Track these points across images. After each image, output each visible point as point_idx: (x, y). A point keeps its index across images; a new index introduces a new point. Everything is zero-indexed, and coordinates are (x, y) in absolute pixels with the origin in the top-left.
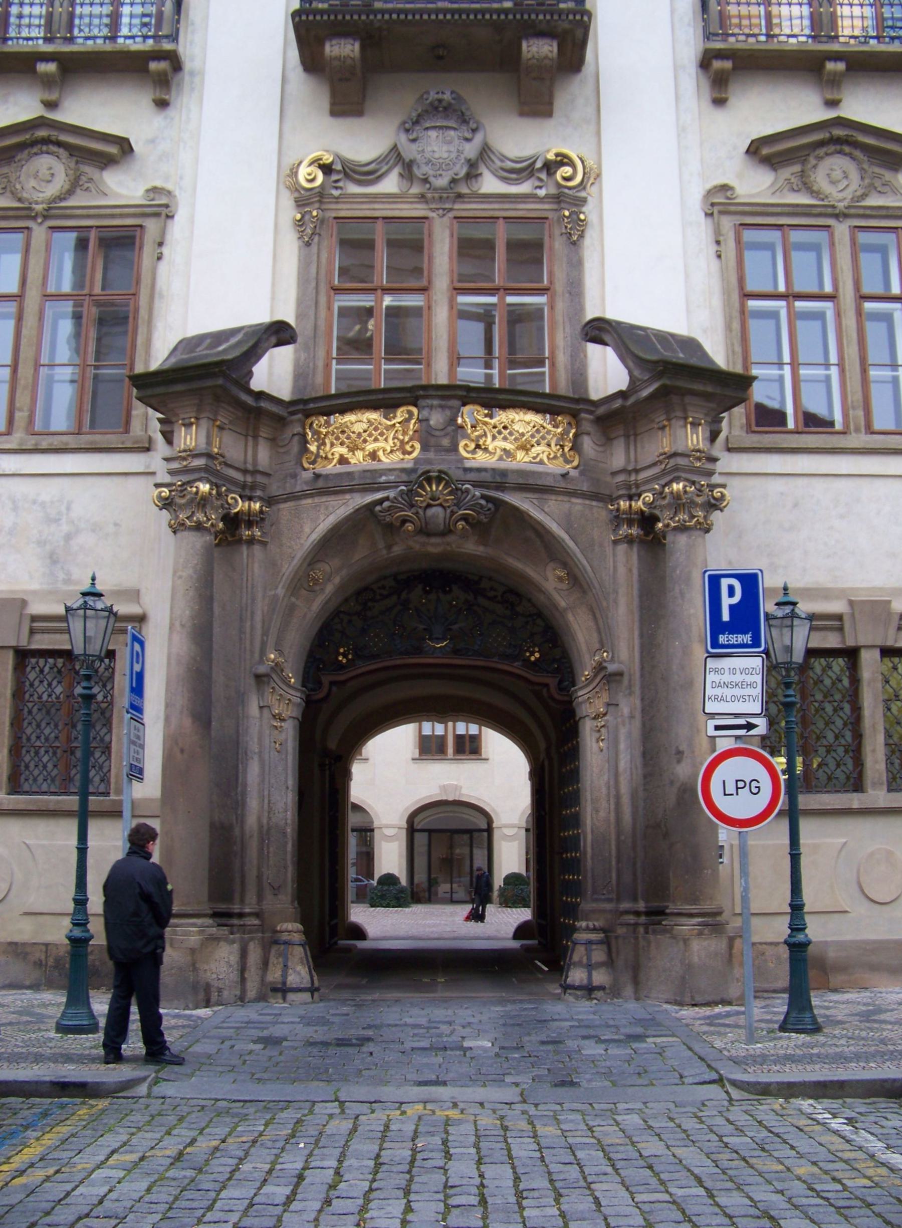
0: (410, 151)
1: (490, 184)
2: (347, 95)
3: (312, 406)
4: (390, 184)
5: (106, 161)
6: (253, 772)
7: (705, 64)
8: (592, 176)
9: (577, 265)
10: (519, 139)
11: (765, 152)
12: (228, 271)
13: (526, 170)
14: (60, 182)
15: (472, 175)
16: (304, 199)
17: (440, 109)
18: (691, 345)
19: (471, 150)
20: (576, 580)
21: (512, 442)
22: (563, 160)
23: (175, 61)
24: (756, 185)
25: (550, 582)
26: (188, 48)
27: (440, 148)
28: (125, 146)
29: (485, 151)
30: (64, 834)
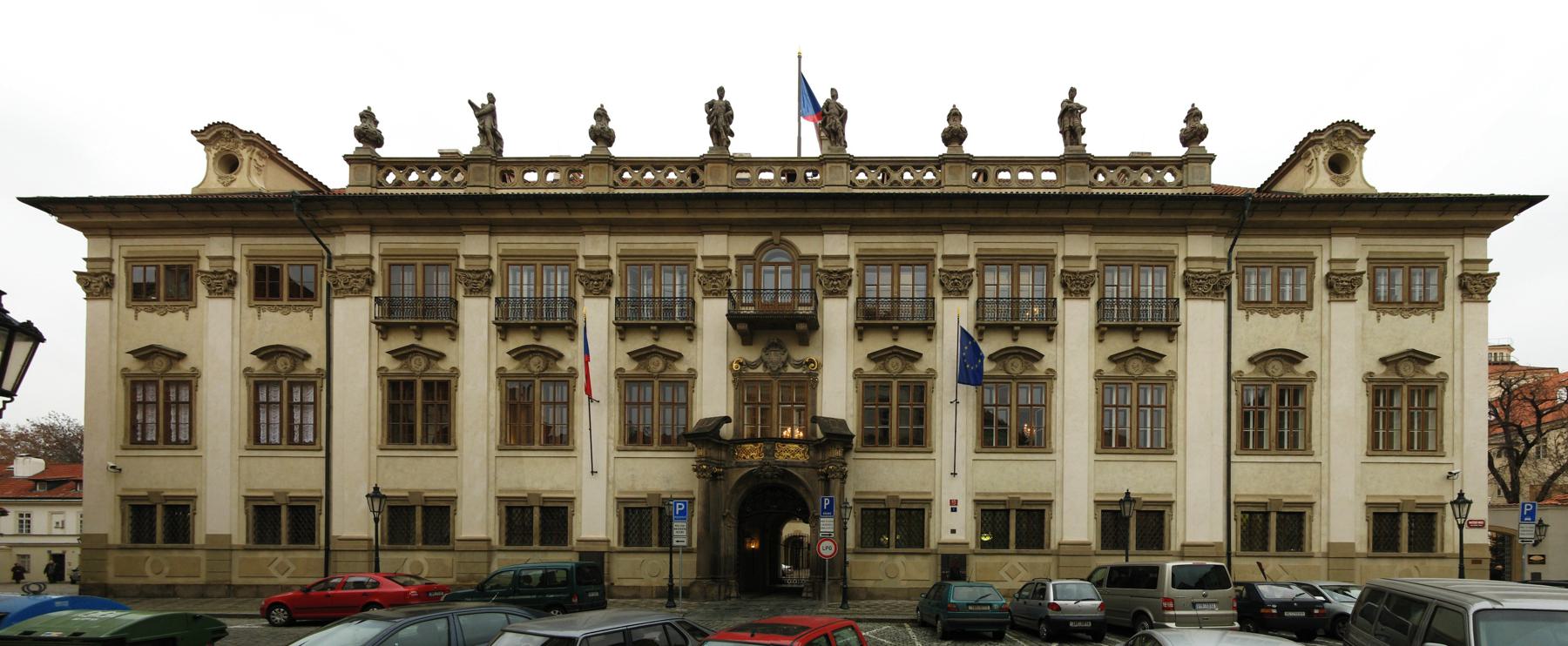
0: (766, 358)
1: (790, 369)
2: (747, 339)
3: (738, 441)
4: (760, 369)
5: (675, 360)
6: (722, 542)
7: (856, 325)
8: (820, 366)
9: (815, 395)
10: (799, 354)
11: (873, 357)
12: (713, 398)
13: (800, 365)
14: (661, 367)
15: (785, 366)
16: (735, 374)
17: (775, 345)
18: (843, 423)
19: (784, 358)
20: (807, 491)
21: (791, 454)
22: (811, 361)
23: (694, 327)
24: (869, 368)
25: (801, 491)
26: (698, 321)
27: (774, 357)
28: (680, 356)
29: (788, 358)
30: (666, 558)
